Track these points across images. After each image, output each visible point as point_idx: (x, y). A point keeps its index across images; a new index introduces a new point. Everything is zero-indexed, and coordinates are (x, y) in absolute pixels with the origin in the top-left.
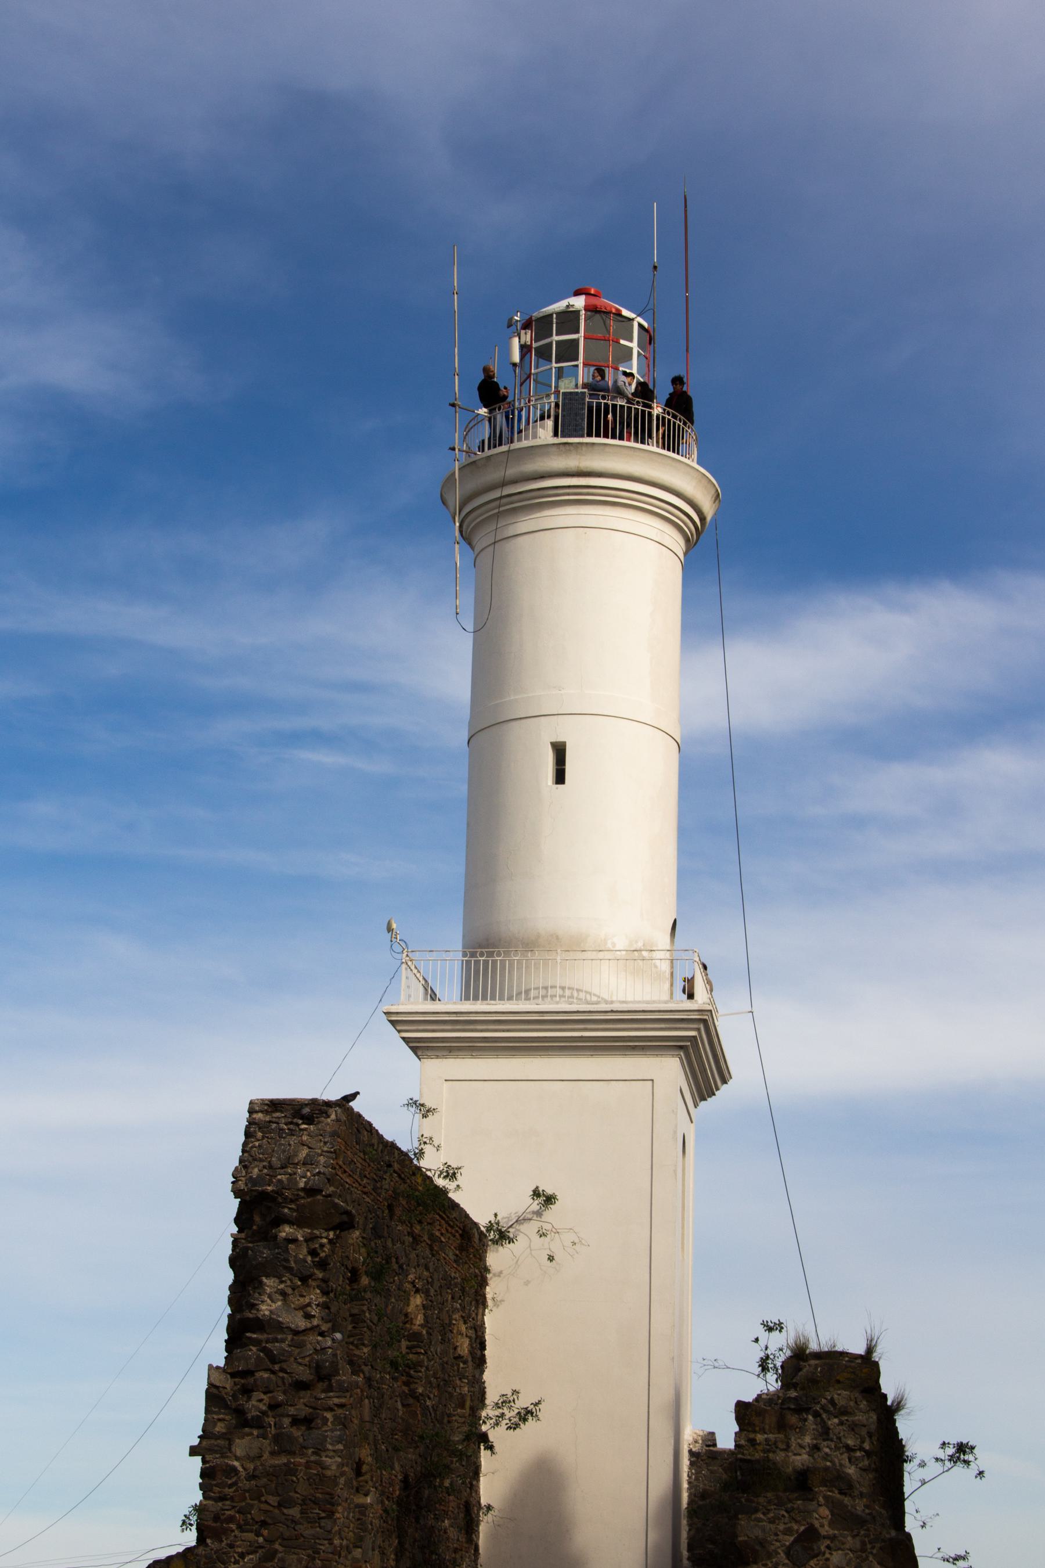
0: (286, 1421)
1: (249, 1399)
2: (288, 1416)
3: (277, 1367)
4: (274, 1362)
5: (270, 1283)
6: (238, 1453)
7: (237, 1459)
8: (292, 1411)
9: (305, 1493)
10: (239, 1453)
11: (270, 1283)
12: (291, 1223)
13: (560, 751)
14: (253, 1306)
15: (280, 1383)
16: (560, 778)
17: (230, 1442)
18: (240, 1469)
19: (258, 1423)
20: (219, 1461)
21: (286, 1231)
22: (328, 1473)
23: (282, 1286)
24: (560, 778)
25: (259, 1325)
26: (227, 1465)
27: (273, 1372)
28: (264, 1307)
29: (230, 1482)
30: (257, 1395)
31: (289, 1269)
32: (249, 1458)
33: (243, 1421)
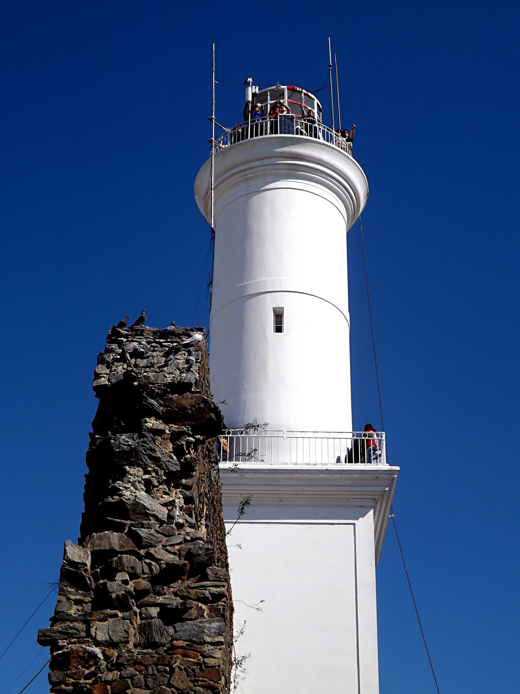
0: (154, 611)
1: (112, 579)
2: (156, 605)
3: (142, 552)
4: (141, 547)
5: (135, 472)
6: (99, 638)
7: (97, 643)
8: (160, 599)
9: (182, 686)
10: (101, 636)
11: (135, 472)
12: (158, 417)
13: (278, 316)
14: (116, 491)
15: (147, 570)
16: (279, 329)
17: (88, 624)
18: (101, 656)
19: (122, 604)
20: (74, 647)
21: (151, 423)
22: (211, 662)
23: (147, 476)
24: (279, 329)
25: (123, 509)
26: (85, 651)
27: (140, 558)
28: (127, 493)
29: (87, 672)
30: (120, 576)
31: (156, 460)
32: (112, 644)
33: (103, 601)
